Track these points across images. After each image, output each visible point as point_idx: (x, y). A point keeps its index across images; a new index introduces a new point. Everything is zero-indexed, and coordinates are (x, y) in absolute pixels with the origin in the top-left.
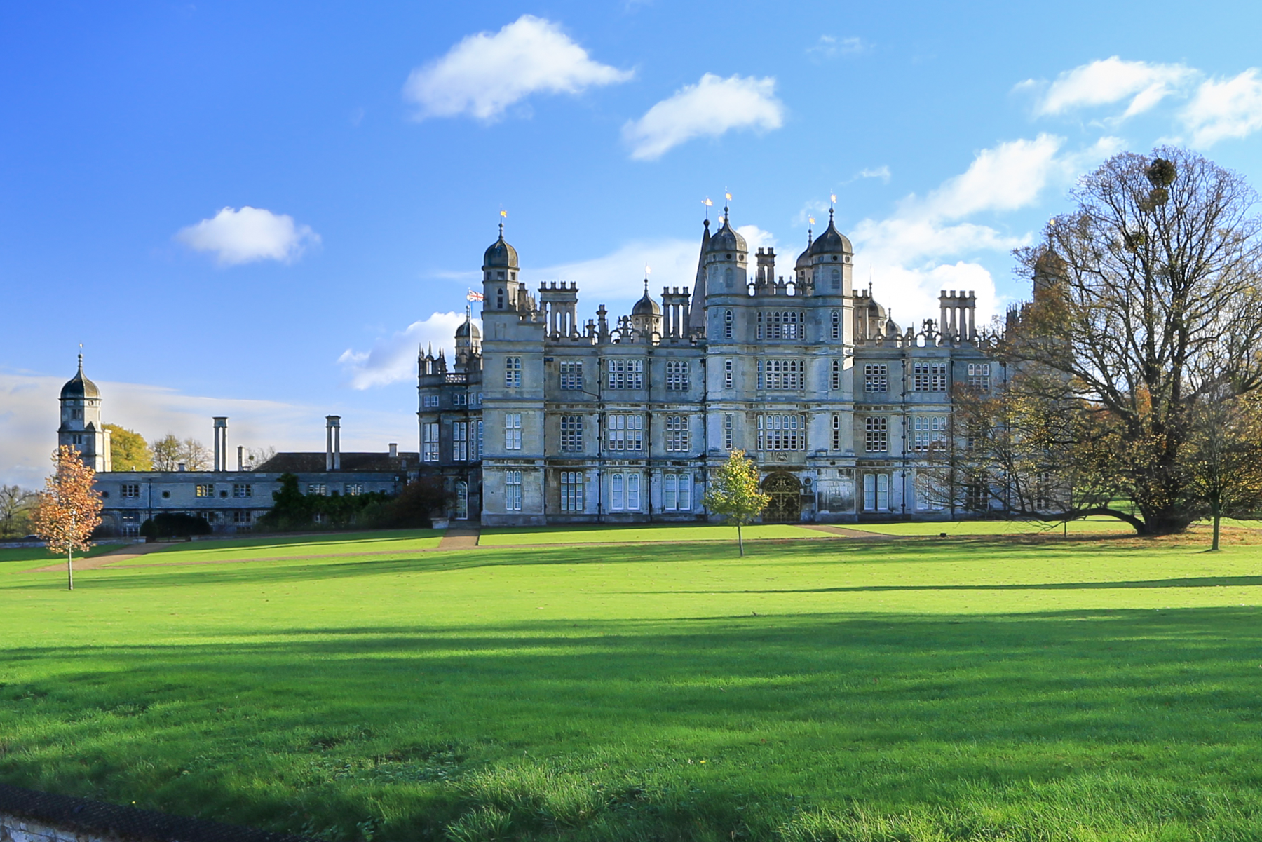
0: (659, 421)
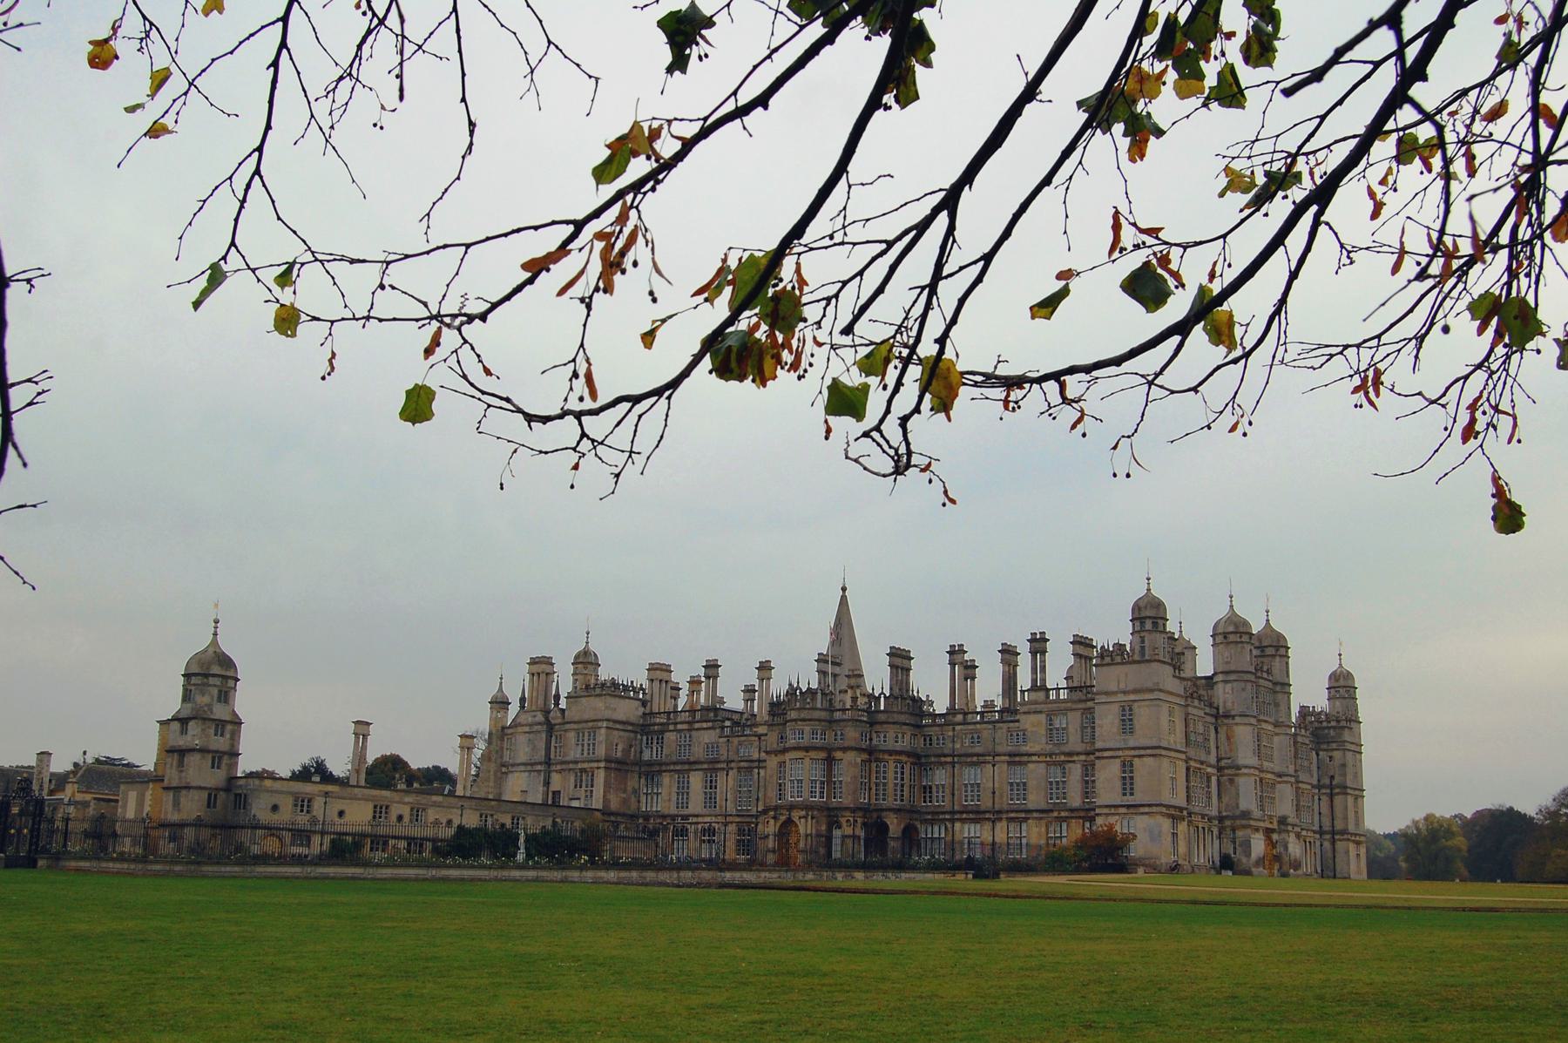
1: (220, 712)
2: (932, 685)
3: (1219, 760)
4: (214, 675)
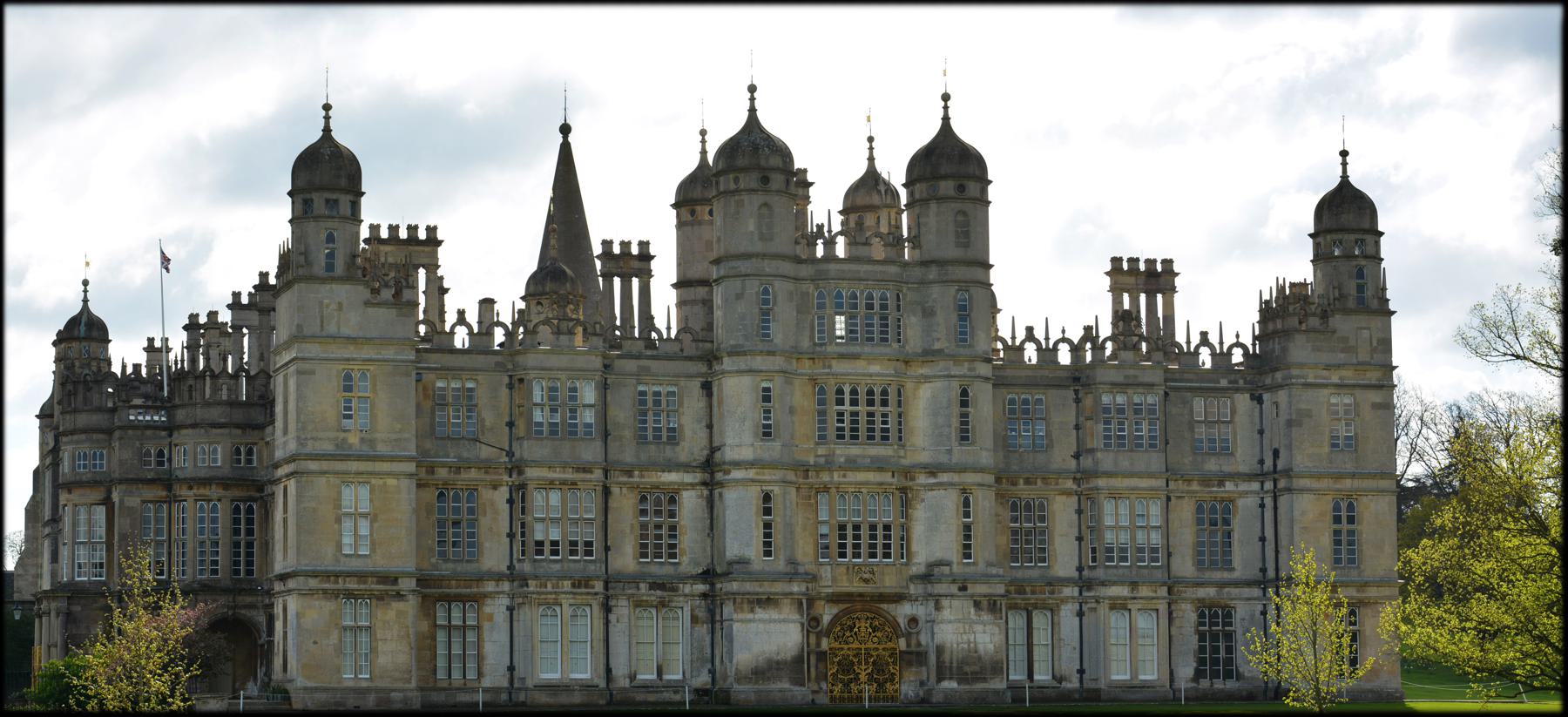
0: (625, 503)
3: (713, 450)
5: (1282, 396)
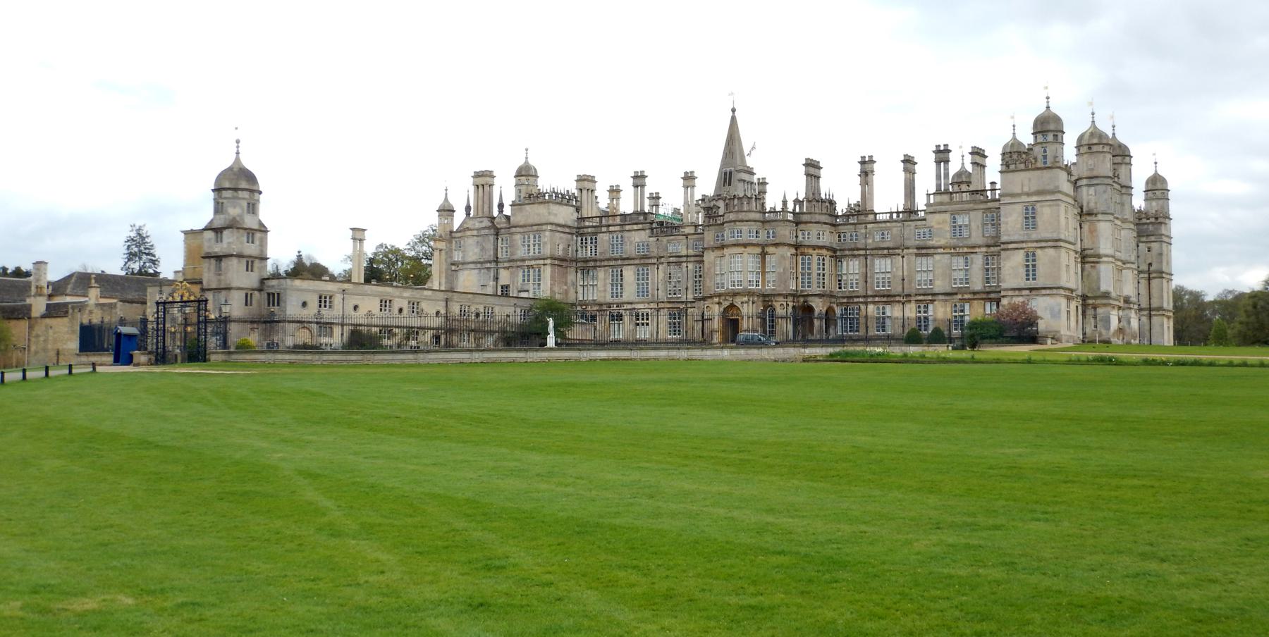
1: (249, 222)
2: (842, 190)
3: (1083, 250)
4: (243, 190)
5: (1155, 246)
